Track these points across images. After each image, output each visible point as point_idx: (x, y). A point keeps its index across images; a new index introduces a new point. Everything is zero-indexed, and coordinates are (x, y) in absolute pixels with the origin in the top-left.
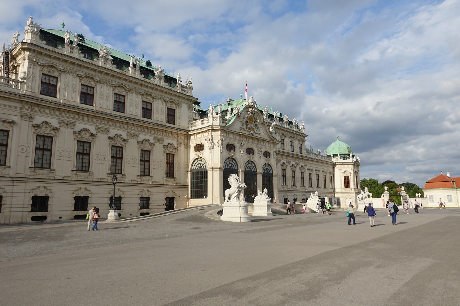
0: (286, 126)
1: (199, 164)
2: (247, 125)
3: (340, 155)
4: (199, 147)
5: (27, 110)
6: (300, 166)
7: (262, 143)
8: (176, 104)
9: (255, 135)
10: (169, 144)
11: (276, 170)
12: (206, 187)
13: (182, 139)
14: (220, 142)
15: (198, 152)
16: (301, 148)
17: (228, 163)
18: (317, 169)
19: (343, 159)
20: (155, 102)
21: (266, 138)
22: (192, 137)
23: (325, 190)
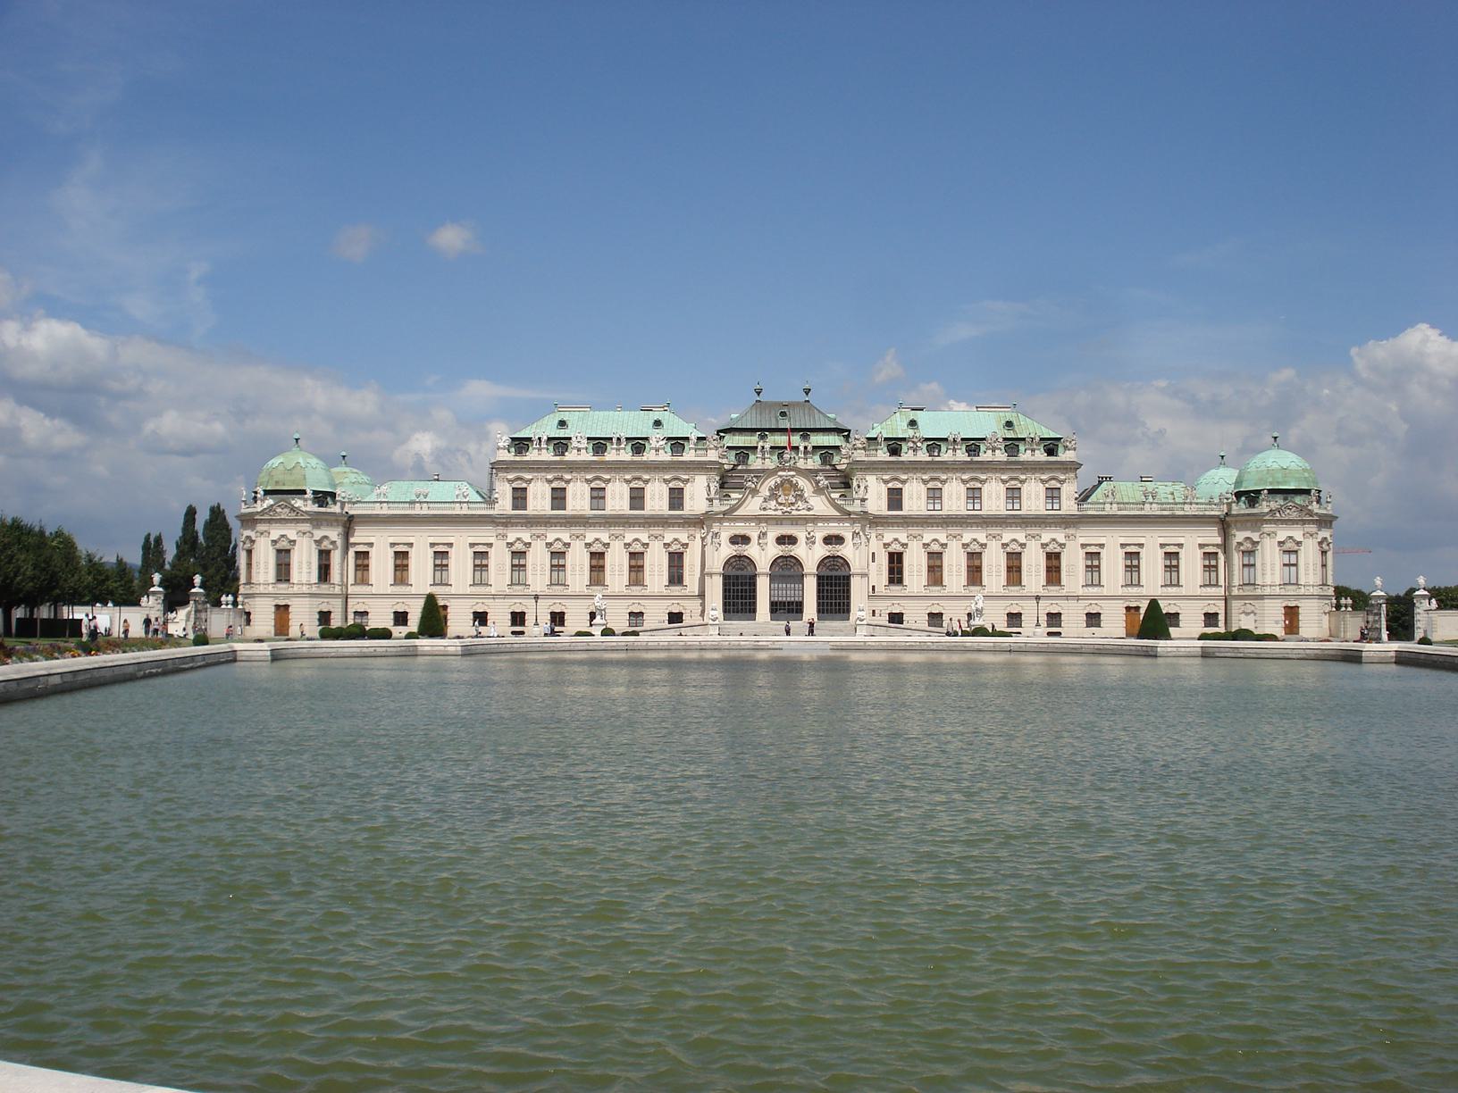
3: (1238, 495)
5: (500, 530)
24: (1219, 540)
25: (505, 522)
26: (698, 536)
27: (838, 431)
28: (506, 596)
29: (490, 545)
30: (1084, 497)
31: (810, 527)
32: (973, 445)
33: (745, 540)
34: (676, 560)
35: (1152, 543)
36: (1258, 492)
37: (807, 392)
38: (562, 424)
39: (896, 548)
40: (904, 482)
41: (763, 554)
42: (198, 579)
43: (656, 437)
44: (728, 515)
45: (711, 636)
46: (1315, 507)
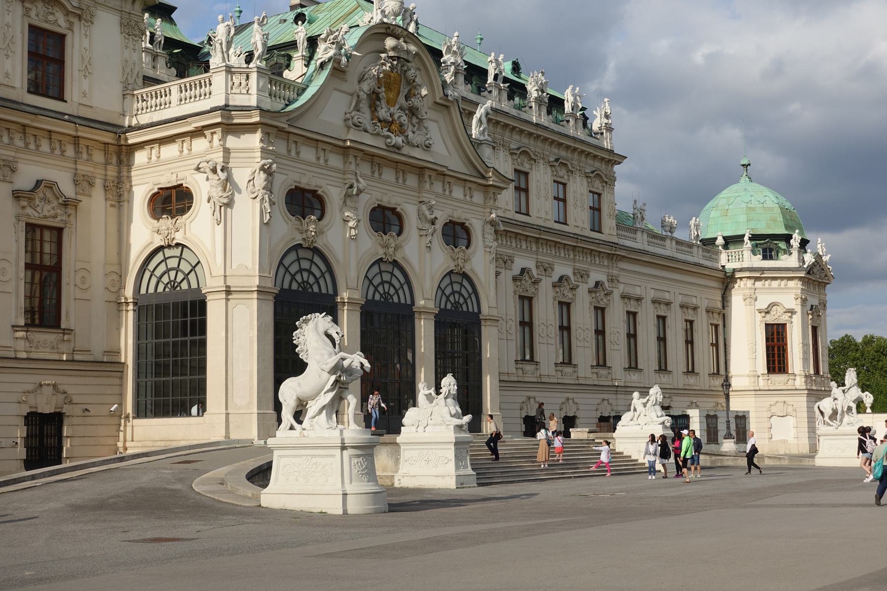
0: (537, 116)
1: (168, 271)
2: (373, 108)
4: (172, 201)
6: (591, 284)
7: (438, 187)
8: (67, 13)
9: (406, 150)
10: (39, 183)
11: (495, 300)
12: (201, 367)
13: (96, 165)
14: (261, 179)
15: (166, 222)
16: (596, 210)
17: (294, 269)
18: (659, 295)
19: (765, 258)
20: (76, 28)
21: (455, 164)
22: (140, 157)
23: (691, 380)
24: (720, 305)
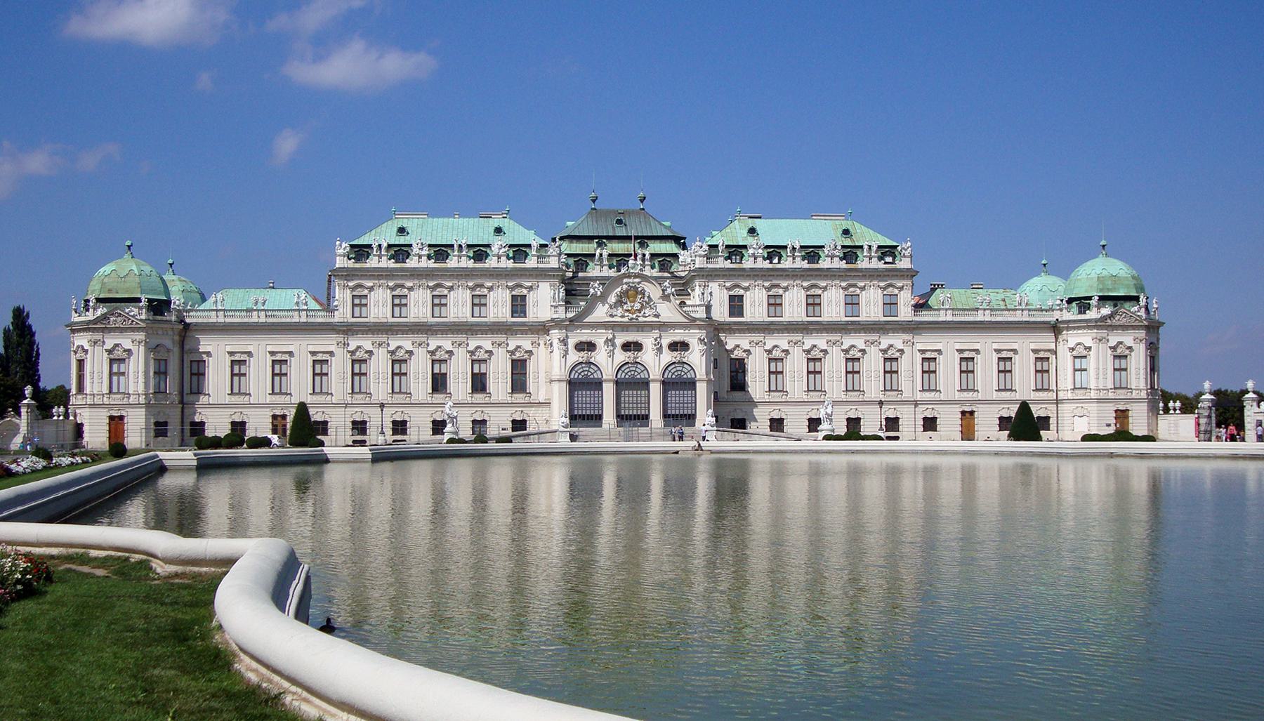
3: (1070, 301)
5: (340, 338)
25: (348, 330)
26: (542, 343)
27: (677, 239)
28: (346, 405)
29: (331, 353)
30: (920, 307)
31: (656, 333)
32: (812, 253)
33: (591, 346)
34: (519, 369)
35: (987, 347)
36: (1090, 298)
37: (643, 200)
38: (402, 231)
39: (738, 354)
40: (746, 289)
41: (607, 362)
42: (28, 390)
43: (497, 244)
44: (572, 324)
45: (564, 442)
46: (1142, 313)
